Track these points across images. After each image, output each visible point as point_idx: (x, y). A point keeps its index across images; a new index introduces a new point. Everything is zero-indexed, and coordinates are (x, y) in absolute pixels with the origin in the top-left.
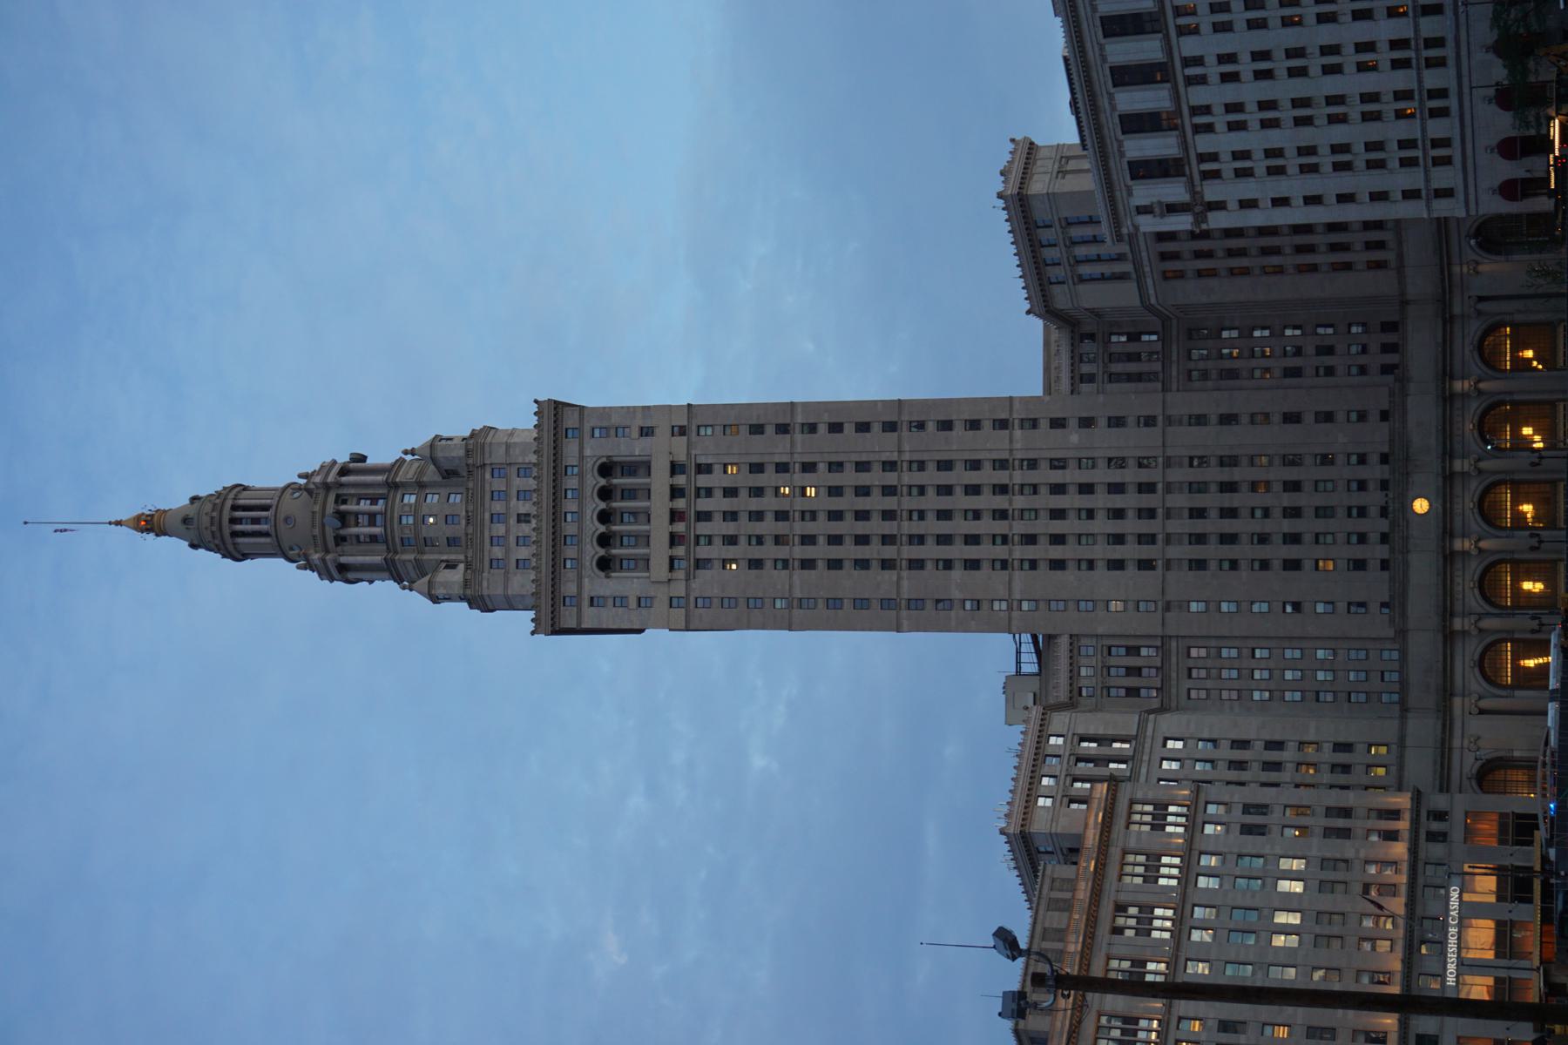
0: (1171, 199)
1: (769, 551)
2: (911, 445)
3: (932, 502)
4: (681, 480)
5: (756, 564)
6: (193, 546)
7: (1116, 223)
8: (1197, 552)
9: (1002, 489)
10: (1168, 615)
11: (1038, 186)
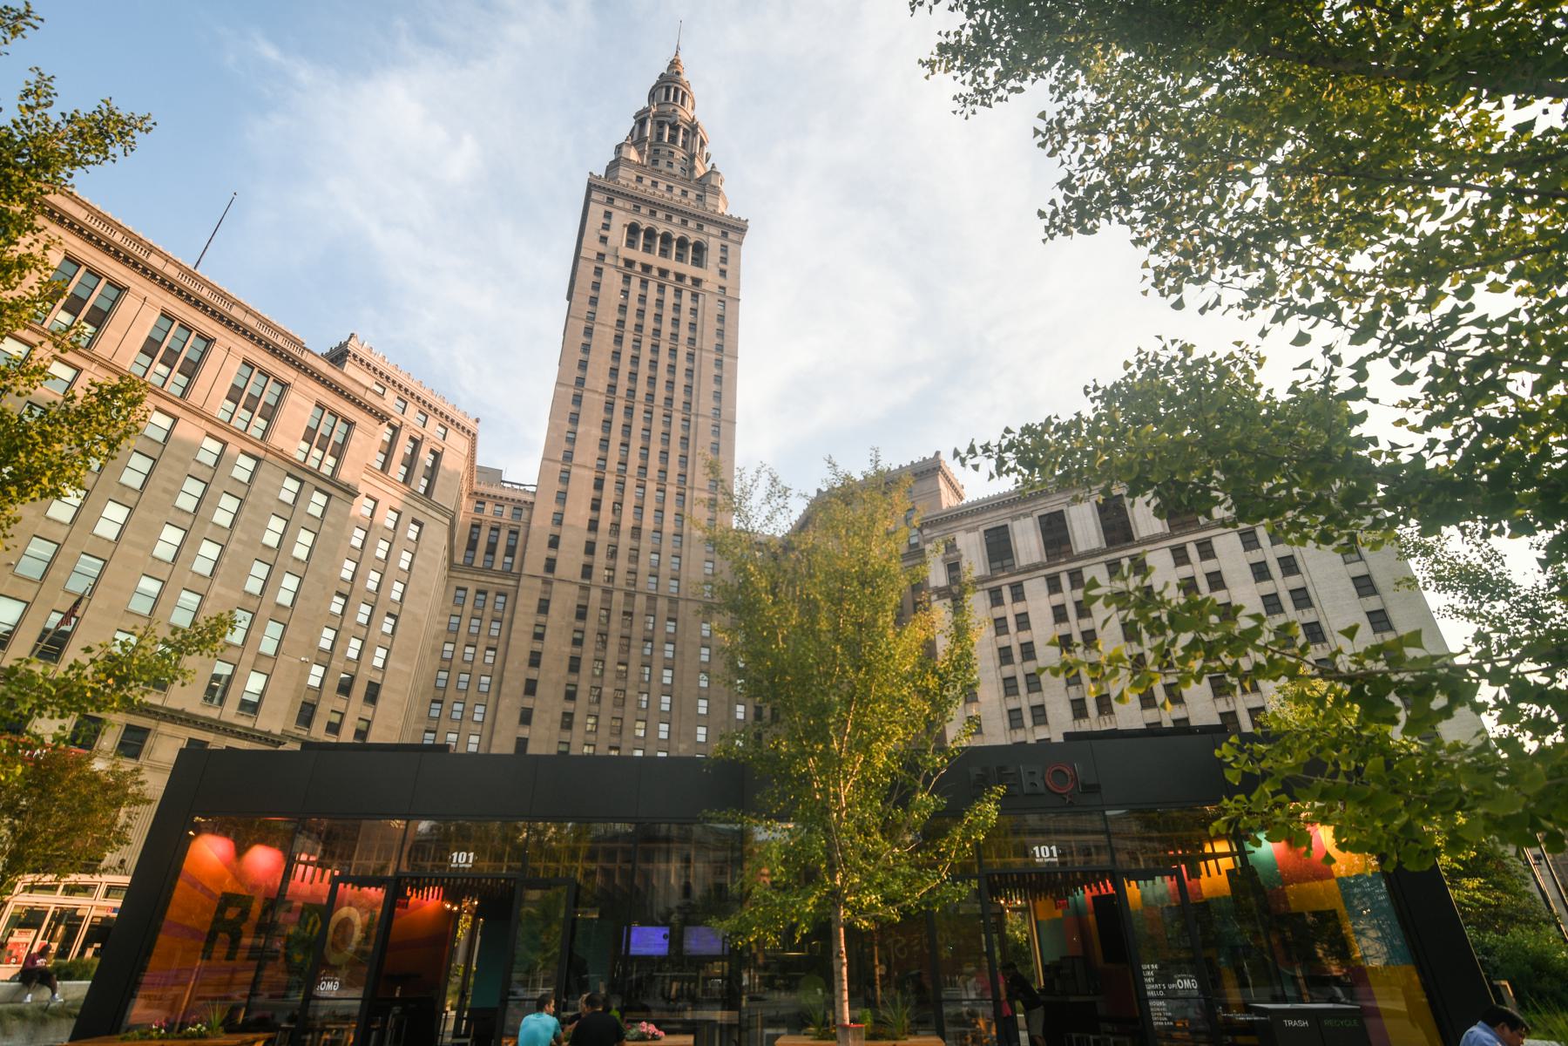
0: (964, 564)
1: (631, 320)
5: (623, 308)
10: (539, 581)
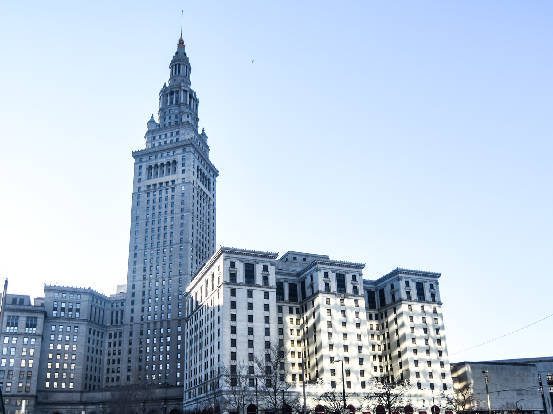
1: (151, 212)
10: (129, 326)
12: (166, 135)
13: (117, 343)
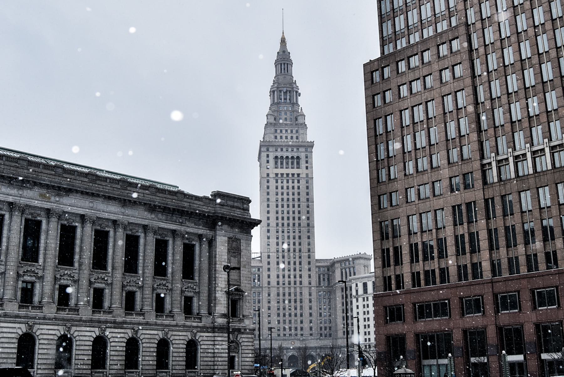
1: (280, 197)
2: (304, 230)
3: (291, 234)
4: (296, 176)
6: (278, 53)
7: (353, 279)
8: (281, 294)
9: (294, 251)
11: (362, 261)
12: (286, 131)
13: (257, 301)
